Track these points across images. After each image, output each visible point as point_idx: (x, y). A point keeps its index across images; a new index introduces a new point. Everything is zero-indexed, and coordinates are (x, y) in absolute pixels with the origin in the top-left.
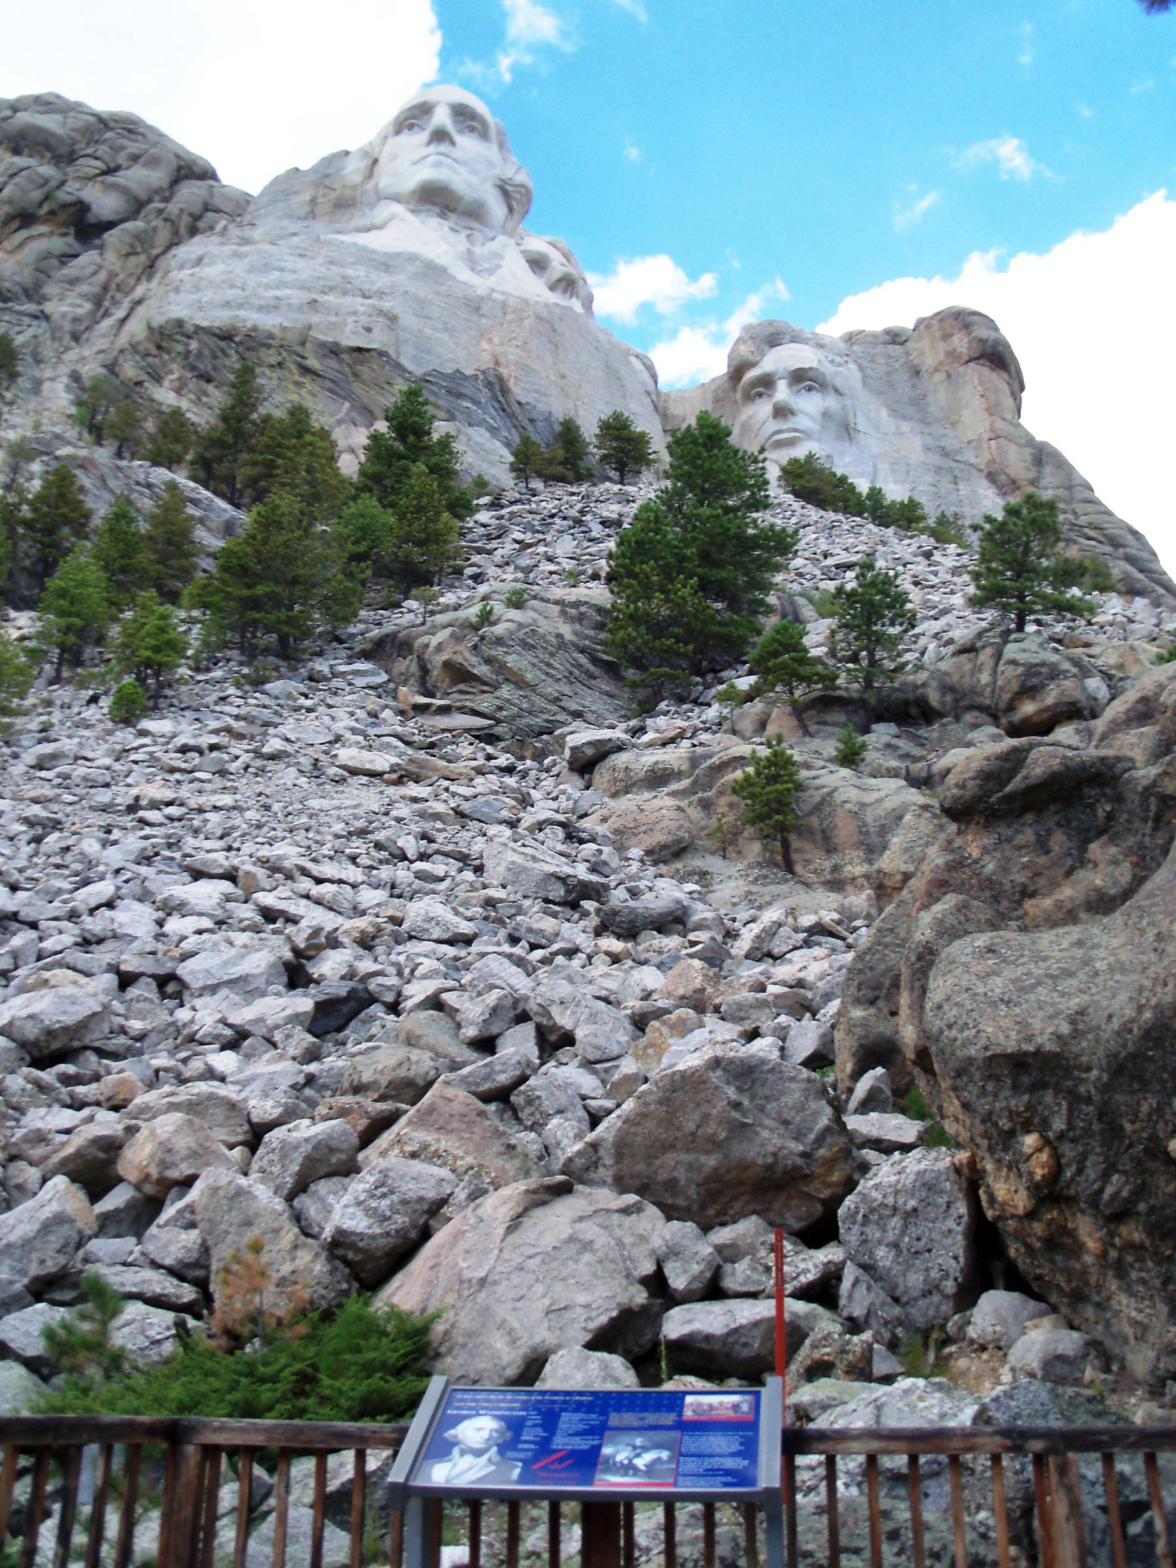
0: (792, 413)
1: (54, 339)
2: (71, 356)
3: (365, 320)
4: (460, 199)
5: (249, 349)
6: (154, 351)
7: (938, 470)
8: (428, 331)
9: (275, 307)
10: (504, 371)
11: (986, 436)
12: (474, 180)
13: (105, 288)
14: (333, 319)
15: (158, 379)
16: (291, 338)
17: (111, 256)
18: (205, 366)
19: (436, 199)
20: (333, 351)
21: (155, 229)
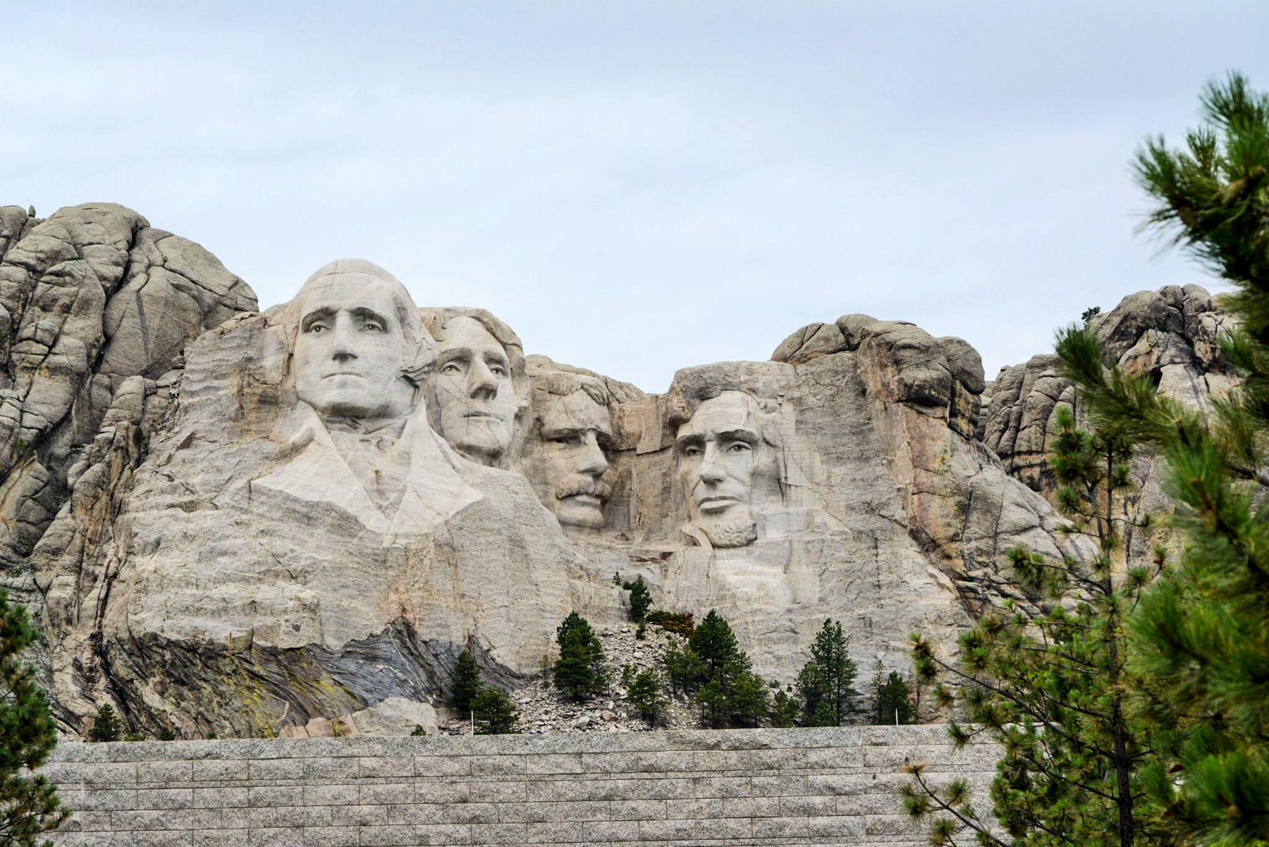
0: (720, 481)
1: (53, 625)
2: (70, 642)
3: (292, 617)
4: (367, 410)
5: (209, 658)
6: (136, 652)
7: (858, 535)
8: (345, 603)
9: (225, 610)
10: (409, 616)
11: (911, 489)
12: (378, 388)
13: (82, 551)
14: (270, 621)
15: (144, 678)
16: (240, 645)
17: (79, 513)
19: (345, 415)
21: (109, 465)
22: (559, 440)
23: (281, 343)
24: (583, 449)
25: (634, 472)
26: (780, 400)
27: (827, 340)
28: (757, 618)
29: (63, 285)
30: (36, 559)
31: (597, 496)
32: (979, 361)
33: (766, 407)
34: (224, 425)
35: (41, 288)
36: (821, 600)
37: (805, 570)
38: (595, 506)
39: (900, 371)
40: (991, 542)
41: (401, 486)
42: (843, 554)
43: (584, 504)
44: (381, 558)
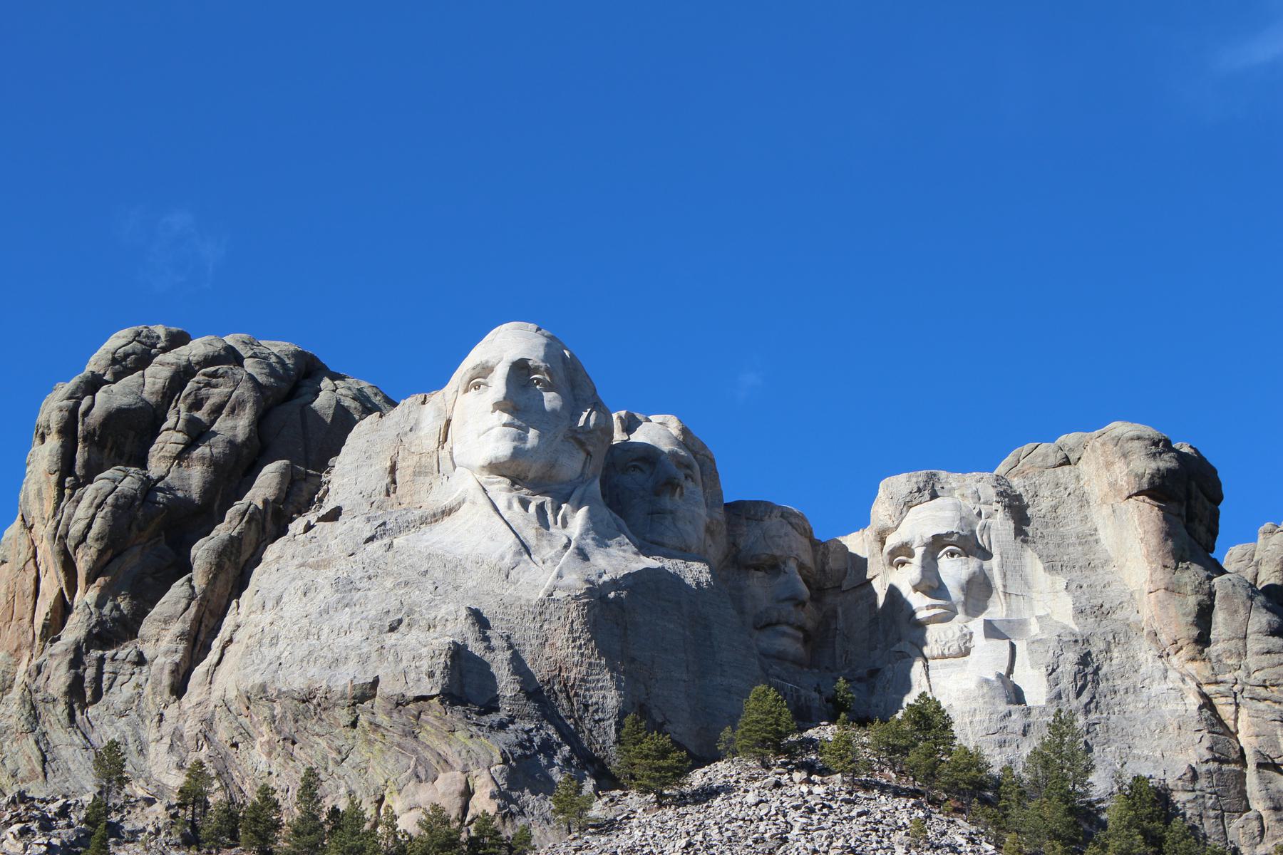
18: (289, 728)
20: (400, 703)
22: (757, 569)
23: (439, 409)
24: (782, 579)
25: (840, 610)
26: (995, 506)
27: (1046, 456)
28: (978, 718)
29: (216, 386)
30: (147, 628)
31: (801, 628)
32: (1214, 471)
33: (980, 514)
34: (373, 499)
35: (190, 386)
36: (1050, 701)
37: (1030, 672)
38: (796, 639)
39: (1128, 464)
40: (1241, 644)
41: (565, 540)
42: (1071, 656)
43: (784, 634)
44: (538, 610)
